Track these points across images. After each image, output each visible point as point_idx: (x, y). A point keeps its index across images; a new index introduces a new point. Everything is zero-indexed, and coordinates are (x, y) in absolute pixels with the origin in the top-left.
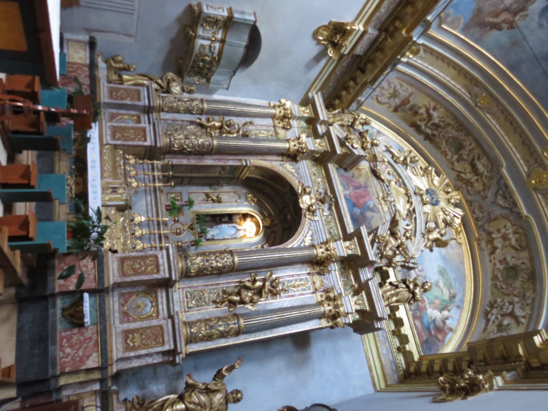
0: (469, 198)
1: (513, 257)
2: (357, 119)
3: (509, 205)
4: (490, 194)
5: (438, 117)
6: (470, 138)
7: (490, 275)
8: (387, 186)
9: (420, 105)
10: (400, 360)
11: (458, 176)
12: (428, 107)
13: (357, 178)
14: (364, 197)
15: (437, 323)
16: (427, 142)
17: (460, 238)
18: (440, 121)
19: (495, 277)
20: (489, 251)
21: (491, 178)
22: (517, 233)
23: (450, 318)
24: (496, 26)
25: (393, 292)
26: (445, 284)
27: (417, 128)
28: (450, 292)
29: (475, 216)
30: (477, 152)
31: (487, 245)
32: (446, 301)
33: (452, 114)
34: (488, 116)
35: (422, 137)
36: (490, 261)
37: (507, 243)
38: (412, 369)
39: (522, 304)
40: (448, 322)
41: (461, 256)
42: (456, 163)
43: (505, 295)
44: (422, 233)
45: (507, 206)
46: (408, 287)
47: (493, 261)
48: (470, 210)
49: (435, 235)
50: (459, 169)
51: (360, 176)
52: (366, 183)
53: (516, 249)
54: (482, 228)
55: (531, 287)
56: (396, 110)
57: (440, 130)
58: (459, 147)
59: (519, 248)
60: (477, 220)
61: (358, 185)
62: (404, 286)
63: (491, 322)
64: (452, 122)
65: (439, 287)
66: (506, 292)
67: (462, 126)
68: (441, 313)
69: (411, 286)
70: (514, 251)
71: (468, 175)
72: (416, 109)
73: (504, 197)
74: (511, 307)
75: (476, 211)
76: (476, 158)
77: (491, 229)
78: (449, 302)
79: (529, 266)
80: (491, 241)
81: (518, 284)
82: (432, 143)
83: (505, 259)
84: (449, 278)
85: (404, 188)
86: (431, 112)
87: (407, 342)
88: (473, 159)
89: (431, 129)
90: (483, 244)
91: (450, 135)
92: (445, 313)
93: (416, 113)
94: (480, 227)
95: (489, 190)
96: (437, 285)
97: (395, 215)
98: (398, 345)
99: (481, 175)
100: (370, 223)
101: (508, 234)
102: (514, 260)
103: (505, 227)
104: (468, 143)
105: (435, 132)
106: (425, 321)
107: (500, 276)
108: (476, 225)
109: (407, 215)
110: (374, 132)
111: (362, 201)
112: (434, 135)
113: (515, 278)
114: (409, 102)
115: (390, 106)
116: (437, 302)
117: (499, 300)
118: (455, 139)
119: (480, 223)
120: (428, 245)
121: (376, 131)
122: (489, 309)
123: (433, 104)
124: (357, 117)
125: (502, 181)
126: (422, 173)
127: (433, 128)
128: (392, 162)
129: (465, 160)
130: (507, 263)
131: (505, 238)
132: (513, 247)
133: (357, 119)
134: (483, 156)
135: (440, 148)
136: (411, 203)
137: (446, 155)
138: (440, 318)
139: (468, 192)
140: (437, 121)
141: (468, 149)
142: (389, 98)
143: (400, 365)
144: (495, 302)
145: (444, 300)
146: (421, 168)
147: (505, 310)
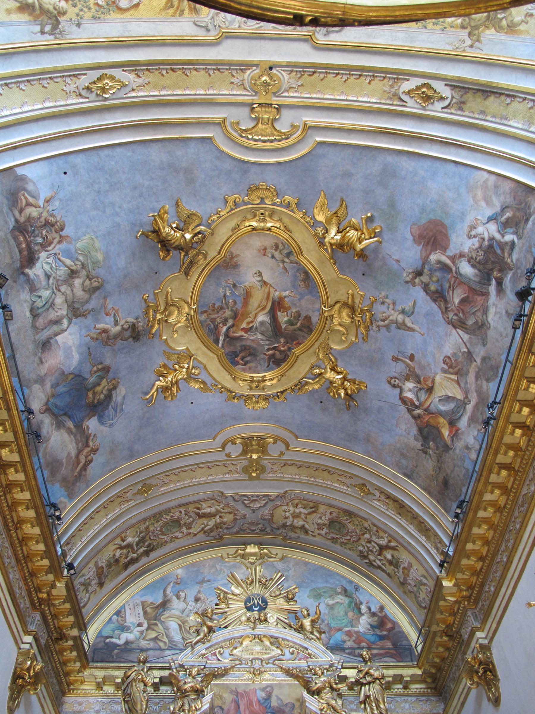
0: (235, 529)
1: (321, 518)
2: (142, 678)
3: (264, 500)
4: (243, 511)
5: (134, 537)
6: (172, 511)
7: (329, 543)
8: (239, 664)
9: (111, 556)
10: (417, 689)
11: (205, 532)
12: (117, 546)
13: (224, 703)
14: (250, 703)
15: (374, 624)
16: (153, 555)
17: (277, 554)
18: (139, 536)
19: (334, 540)
20: (303, 533)
21: (227, 505)
22: (297, 505)
23: (370, 605)
24: (85, 467)
25: (374, 705)
26: (331, 596)
27: (133, 561)
28: (340, 593)
29: (258, 531)
30: (191, 508)
31: (296, 532)
32: (351, 602)
33: (139, 522)
34: (162, 489)
35: (144, 560)
36: (315, 536)
37: (303, 516)
38: (429, 680)
39: (375, 535)
40: (373, 610)
41: (298, 563)
42: (191, 531)
43: (357, 541)
44: (305, 639)
45: (264, 502)
46: (369, 683)
47: (316, 534)
48: (248, 533)
49: (307, 623)
50: (198, 530)
51: (221, 697)
52: (232, 692)
53: (314, 512)
54: (274, 530)
55: (360, 520)
56: (101, 585)
57: (147, 538)
58: (177, 523)
59: (313, 510)
60: (263, 531)
61: (233, 704)
62: (367, 686)
63: (383, 567)
64: (147, 524)
65: (333, 605)
66: (355, 539)
67: (157, 516)
68: (363, 615)
69: (368, 679)
70: (315, 514)
71: (210, 523)
72: (112, 561)
73: (255, 501)
74: (373, 543)
75: (253, 528)
76: (197, 511)
77: (281, 523)
78: (351, 600)
79: (337, 510)
80: (293, 528)
81: (351, 527)
82: (156, 549)
83: (318, 524)
84: (323, 588)
85: (243, 639)
86: (125, 543)
87: (401, 677)
88: (198, 514)
89: (141, 547)
90: (293, 535)
91: (159, 529)
92: (363, 608)
93: (117, 561)
94: (272, 531)
95: (237, 511)
96: (331, 607)
97: (281, 668)
98: (401, 686)
99: (218, 512)
100: (287, 704)
101: (294, 512)
102: (323, 518)
103: (285, 512)
104: (178, 514)
105: (147, 544)
106: (372, 639)
107: (335, 536)
108: (268, 534)
109: (277, 648)
110: (117, 620)
111: (256, 707)
112: (149, 546)
113: (344, 526)
114: (102, 567)
115: (95, 591)
116: (351, 614)
117: (361, 548)
118: (166, 524)
119: (268, 530)
120: (318, 635)
121: (115, 616)
122: (367, 561)
123: (118, 541)
124: (140, 677)
125: (236, 498)
126: (223, 606)
127: (141, 544)
128: (207, 645)
129: (193, 522)
130: (324, 525)
131: (296, 516)
132: (310, 514)
133: (142, 678)
134: (199, 504)
135: (166, 542)
136: (265, 636)
137: (176, 538)
138: (369, 618)
139: (227, 528)
140: (137, 539)
141: (183, 515)
142: (87, 592)
143: (422, 690)
144: (361, 552)
145: (350, 607)
146: (217, 605)
147: (375, 550)
